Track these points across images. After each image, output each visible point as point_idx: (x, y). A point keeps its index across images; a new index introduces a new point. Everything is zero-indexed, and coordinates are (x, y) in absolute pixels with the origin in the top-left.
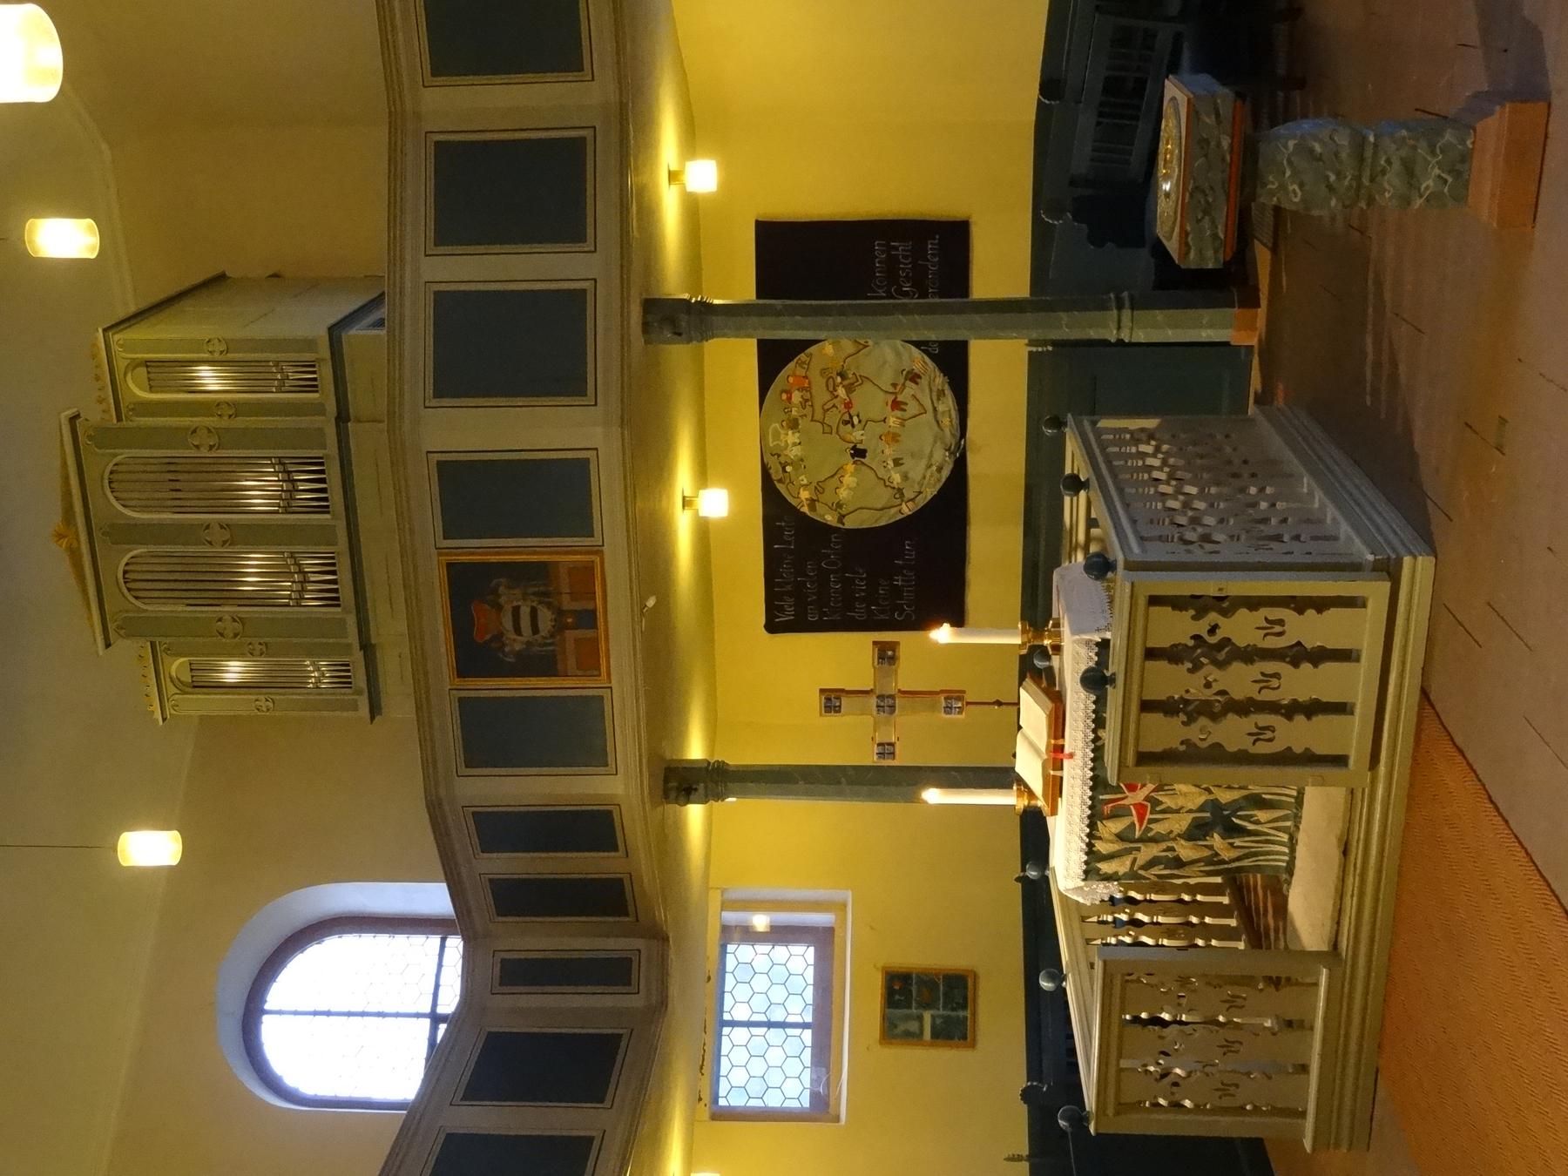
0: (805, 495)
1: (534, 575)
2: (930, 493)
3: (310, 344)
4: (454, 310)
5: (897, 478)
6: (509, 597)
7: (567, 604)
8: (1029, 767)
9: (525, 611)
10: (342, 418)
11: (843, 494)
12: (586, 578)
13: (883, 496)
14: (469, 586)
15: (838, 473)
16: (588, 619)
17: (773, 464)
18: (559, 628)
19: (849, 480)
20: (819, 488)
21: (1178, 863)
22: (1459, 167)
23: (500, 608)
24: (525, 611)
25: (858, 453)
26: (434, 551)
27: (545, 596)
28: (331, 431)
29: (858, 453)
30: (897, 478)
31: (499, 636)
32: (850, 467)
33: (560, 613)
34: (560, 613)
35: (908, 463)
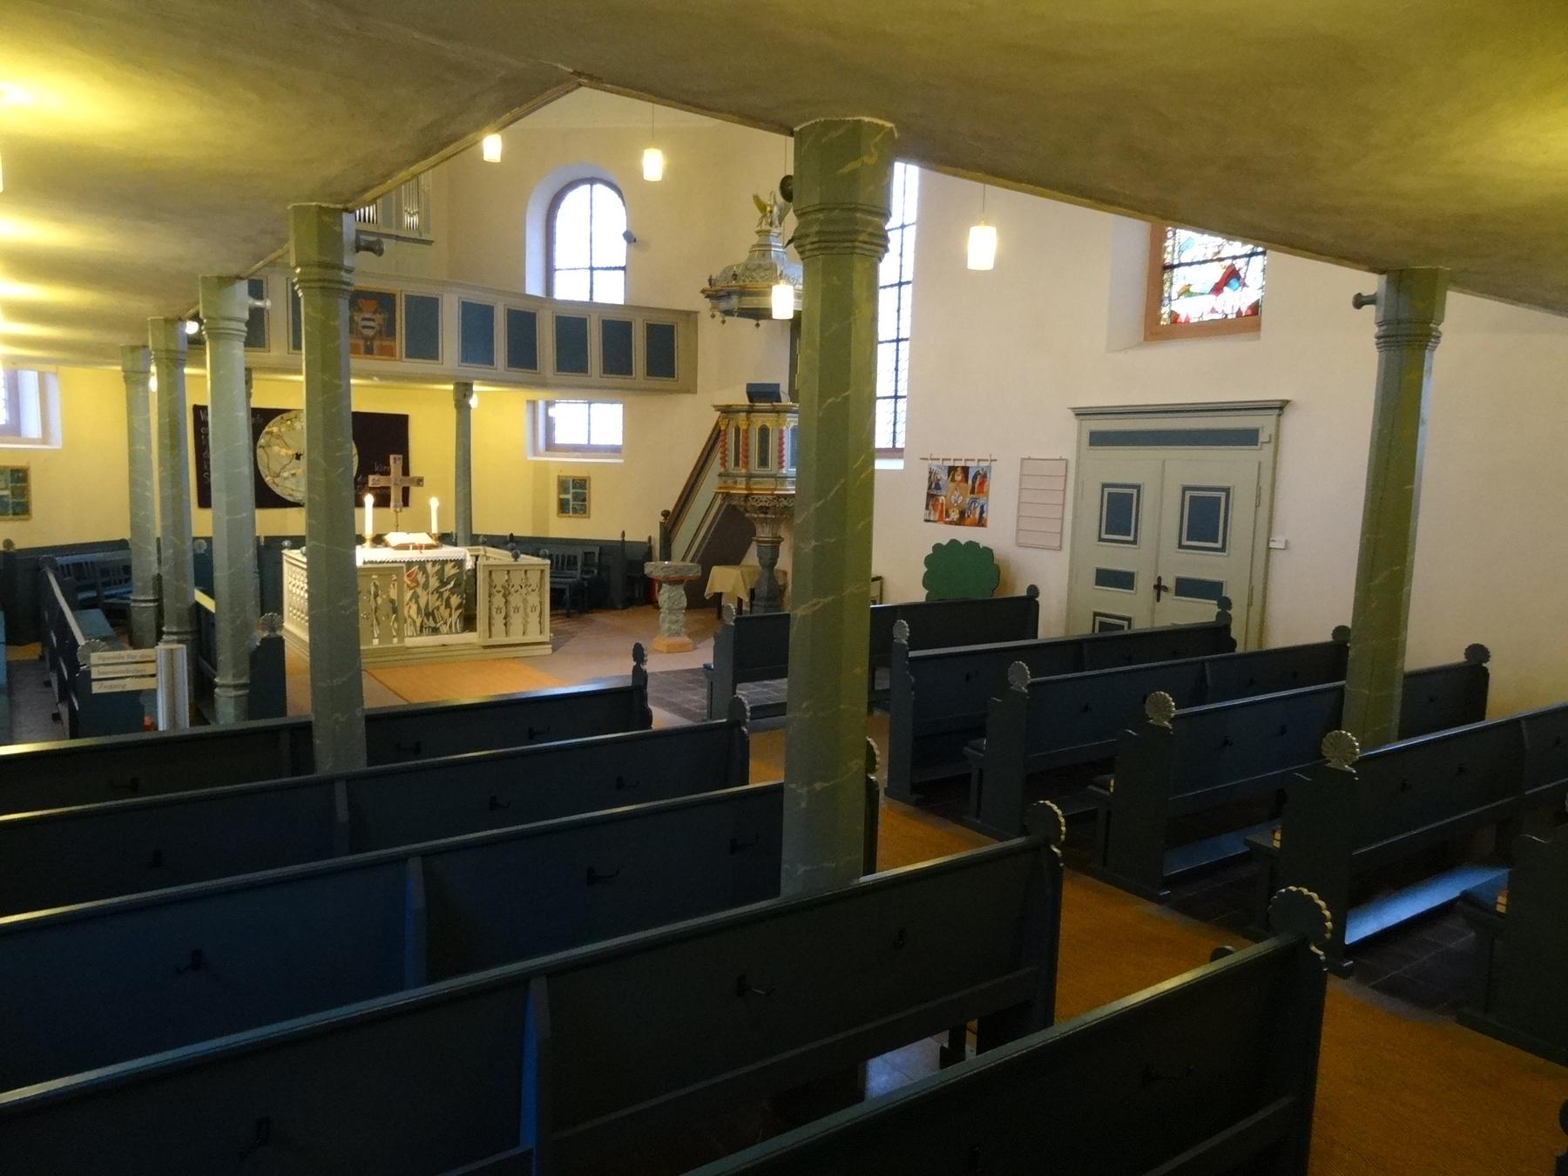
0: (275, 429)
1: (389, 330)
2: (278, 491)
3: (428, 230)
4: (486, 313)
5: (285, 474)
6: (378, 317)
7: (376, 343)
8: (393, 538)
9: (371, 324)
10: (397, 238)
11: (276, 448)
12: (389, 352)
13: (275, 467)
14: (385, 301)
15: (287, 446)
16: (369, 351)
17: (291, 415)
18: (366, 339)
19: (284, 452)
20: (279, 436)
21: (376, 596)
22: (678, 634)
23: (375, 313)
24: (371, 324)
25: (298, 457)
26: (402, 289)
27: (380, 332)
28: (393, 232)
29: (298, 457)
30: (285, 474)
31: (360, 310)
32: (291, 452)
33: (373, 339)
34: (373, 339)
35: (294, 480)
